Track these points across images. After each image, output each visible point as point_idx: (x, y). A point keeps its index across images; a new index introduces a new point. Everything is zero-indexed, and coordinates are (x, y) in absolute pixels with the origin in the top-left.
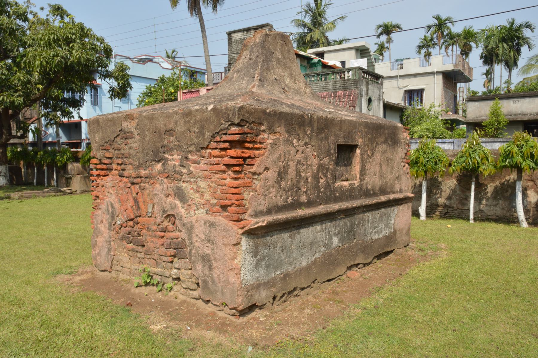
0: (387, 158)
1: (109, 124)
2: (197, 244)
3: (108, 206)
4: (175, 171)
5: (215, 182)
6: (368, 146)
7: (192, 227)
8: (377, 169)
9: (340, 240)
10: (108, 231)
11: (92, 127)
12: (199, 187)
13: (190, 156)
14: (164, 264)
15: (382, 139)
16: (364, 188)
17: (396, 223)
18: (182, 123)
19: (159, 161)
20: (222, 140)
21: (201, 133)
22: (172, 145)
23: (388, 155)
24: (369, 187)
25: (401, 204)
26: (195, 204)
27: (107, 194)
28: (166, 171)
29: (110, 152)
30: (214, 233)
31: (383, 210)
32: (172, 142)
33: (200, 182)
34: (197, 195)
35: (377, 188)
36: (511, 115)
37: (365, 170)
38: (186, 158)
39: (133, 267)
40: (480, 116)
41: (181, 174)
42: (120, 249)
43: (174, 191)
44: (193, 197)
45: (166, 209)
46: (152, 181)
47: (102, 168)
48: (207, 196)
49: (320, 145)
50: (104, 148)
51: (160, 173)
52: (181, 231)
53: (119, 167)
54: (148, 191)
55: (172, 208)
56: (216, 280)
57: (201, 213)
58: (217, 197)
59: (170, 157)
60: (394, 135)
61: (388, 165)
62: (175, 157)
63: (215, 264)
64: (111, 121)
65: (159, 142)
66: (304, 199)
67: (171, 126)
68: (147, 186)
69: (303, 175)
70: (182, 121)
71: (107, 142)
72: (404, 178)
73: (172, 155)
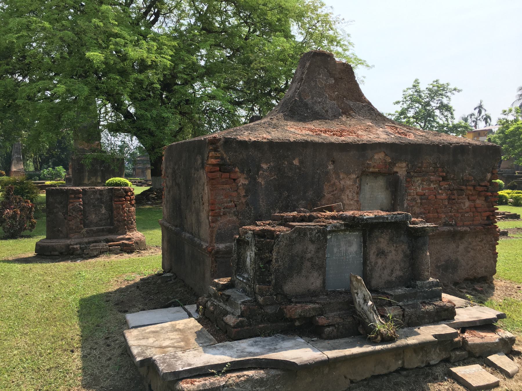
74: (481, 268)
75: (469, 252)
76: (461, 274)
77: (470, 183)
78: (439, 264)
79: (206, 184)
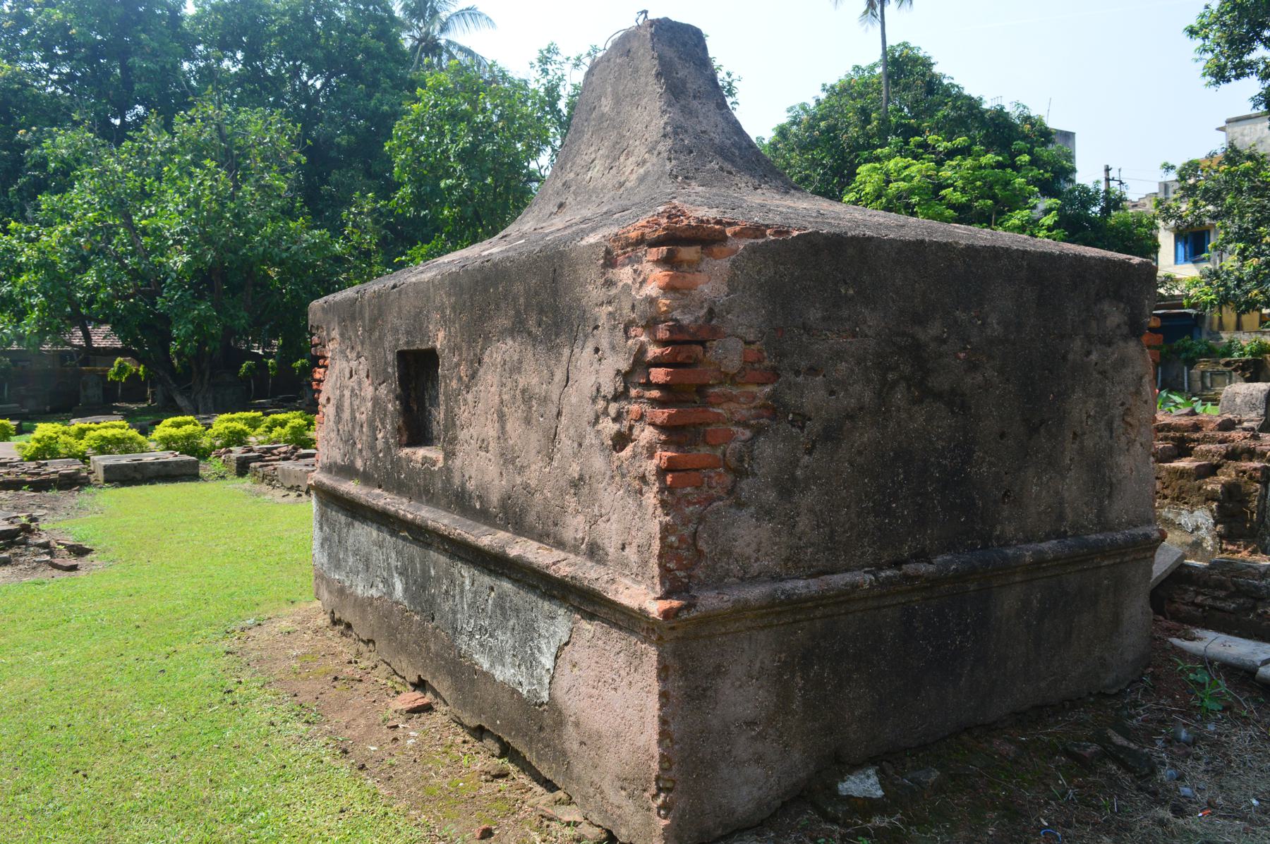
0: (523, 391)
6: (460, 349)
8: (491, 431)
9: (406, 590)
15: (504, 322)
16: (457, 481)
17: (564, 682)
23: (530, 379)
24: (471, 486)
25: (591, 617)
31: (507, 586)
35: (494, 498)
37: (454, 425)
49: (373, 356)
60: (555, 293)
61: (527, 421)
66: (359, 464)
69: (357, 415)
72: (610, 496)
79: (1147, 379)
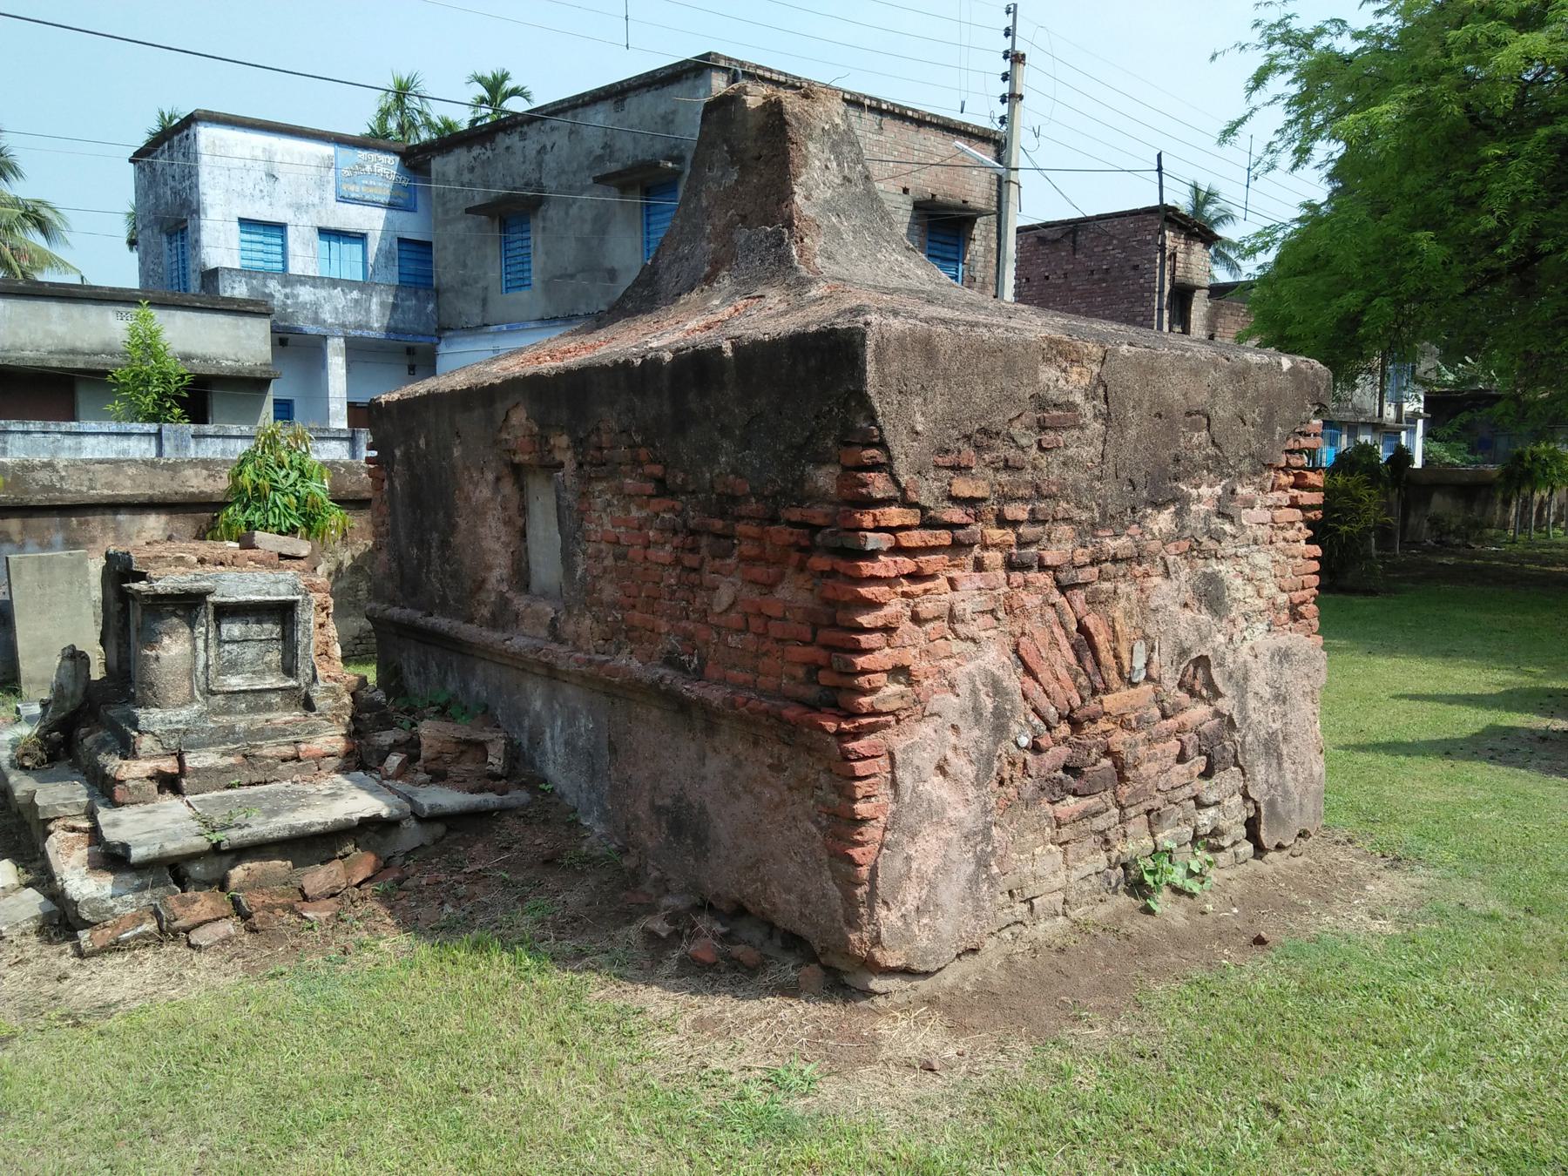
1: (984, 364)
2: (1254, 717)
3: (974, 692)
4: (1209, 531)
5: (1283, 552)
7: (1246, 679)
10: (971, 793)
11: (895, 366)
12: (1254, 567)
13: (1239, 490)
14: (1177, 809)
18: (1229, 396)
19: (1158, 506)
20: (1297, 446)
21: (1267, 427)
22: (1198, 456)
26: (1244, 614)
27: (956, 646)
28: (1187, 533)
29: (973, 477)
30: (1288, 674)
32: (1198, 447)
33: (1257, 555)
34: (1250, 590)
36: (112, 354)
38: (1233, 492)
39: (1075, 875)
40: (14, 348)
41: (1217, 536)
42: (1030, 837)
43: (1195, 589)
44: (1240, 595)
45: (1187, 645)
46: (1138, 570)
47: (933, 542)
48: (1270, 589)
50: (948, 460)
51: (1167, 539)
52: (1218, 694)
53: (1009, 536)
54: (1123, 603)
55: (1203, 639)
56: (1291, 785)
57: (1258, 636)
58: (1286, 586)
59: (1194, 492)
62: (1204, 490)
63: (1285, 750)
64: (992, 352)
65: (1166, 446)
67: (1201, 398)
68: (1123, 587)
70: (1227, 392)
71: (968, 437)
73: (1197, 486)
74: (789, 890)
75: (737, 797)
76: (723, 878)
77: (743, 510)
78: (659, 802)
